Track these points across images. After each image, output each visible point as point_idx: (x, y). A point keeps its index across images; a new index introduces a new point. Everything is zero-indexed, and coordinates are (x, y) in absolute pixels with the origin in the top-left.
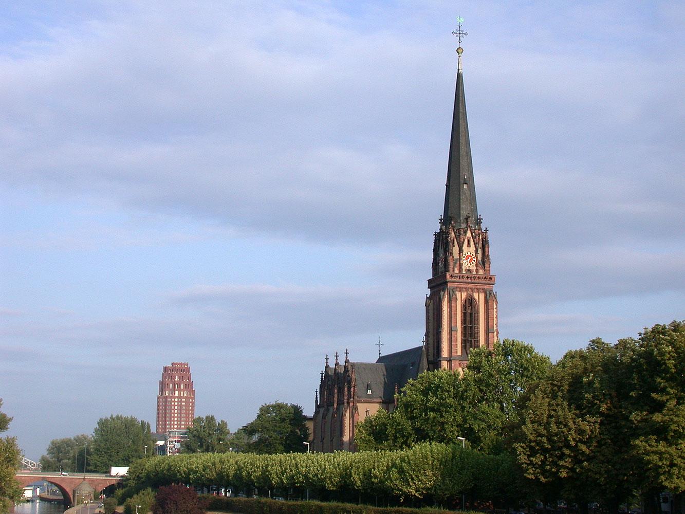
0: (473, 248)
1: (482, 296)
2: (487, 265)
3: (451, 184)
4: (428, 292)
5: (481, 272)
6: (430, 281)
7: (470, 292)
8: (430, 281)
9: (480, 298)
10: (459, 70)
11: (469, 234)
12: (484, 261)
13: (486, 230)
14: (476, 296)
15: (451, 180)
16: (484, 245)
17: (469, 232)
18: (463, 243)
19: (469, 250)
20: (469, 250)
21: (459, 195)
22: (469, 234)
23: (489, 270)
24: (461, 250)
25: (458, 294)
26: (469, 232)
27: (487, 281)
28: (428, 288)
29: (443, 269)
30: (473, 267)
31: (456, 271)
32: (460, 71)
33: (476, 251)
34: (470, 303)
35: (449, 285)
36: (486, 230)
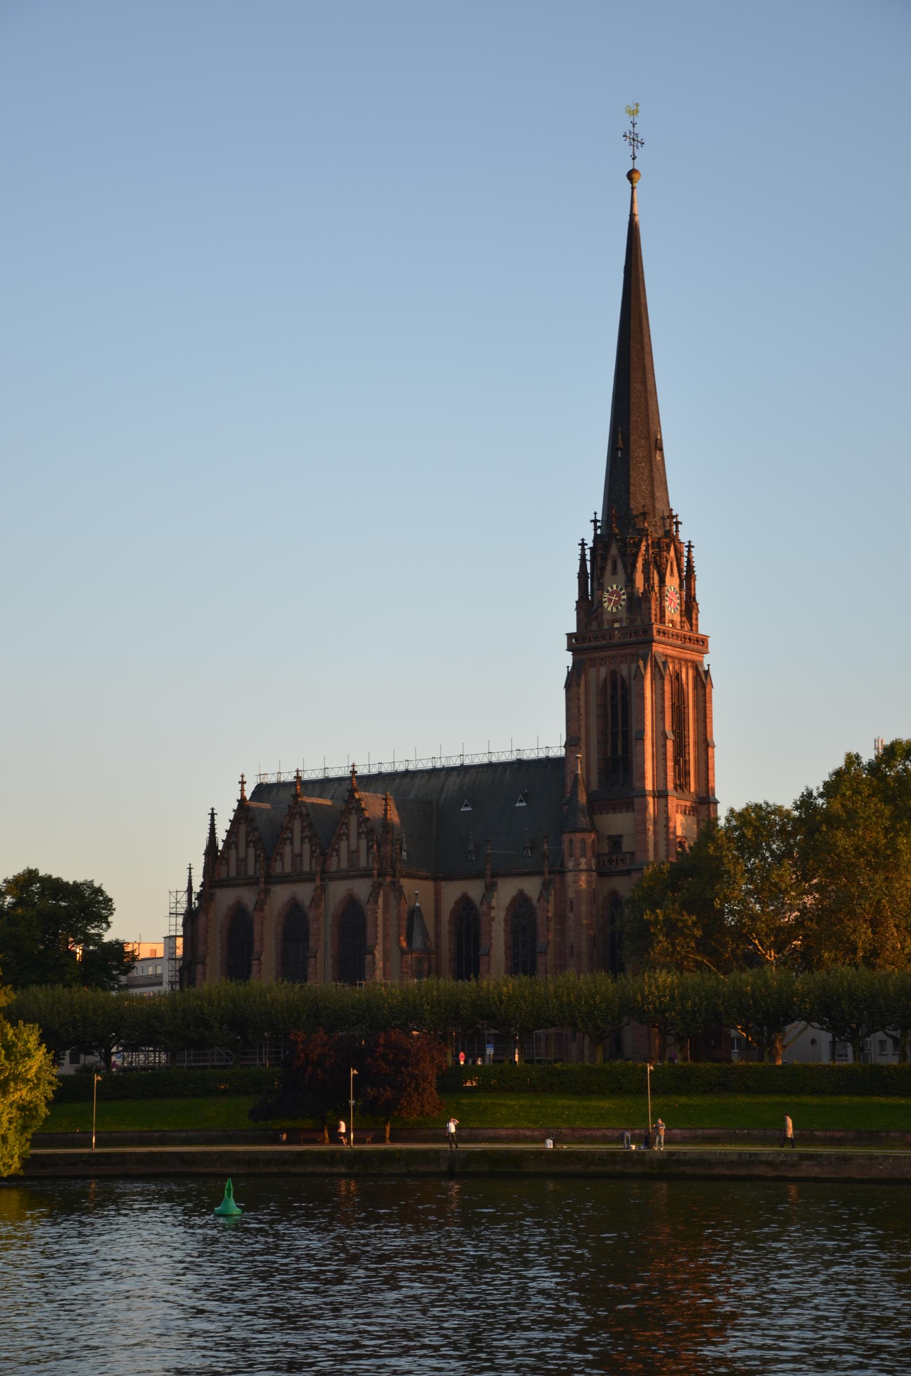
0: (676, 580)
3: (633, 446)
4: (568, 659)
6: (570, 636)
7: (677, 666)
8: (570, 636)
9: (687, 677)
10: (632, 215)
11: (672, 553)
15: (632, 438)
16: (688, 578)
21: (651, 470)
23: (697, 625)
24: (662, 581)
28: (568, 650)
30: (677, 618)
32: (637, 218)
33: (681, 586)
35: (657, 648)
36: (690, 547)
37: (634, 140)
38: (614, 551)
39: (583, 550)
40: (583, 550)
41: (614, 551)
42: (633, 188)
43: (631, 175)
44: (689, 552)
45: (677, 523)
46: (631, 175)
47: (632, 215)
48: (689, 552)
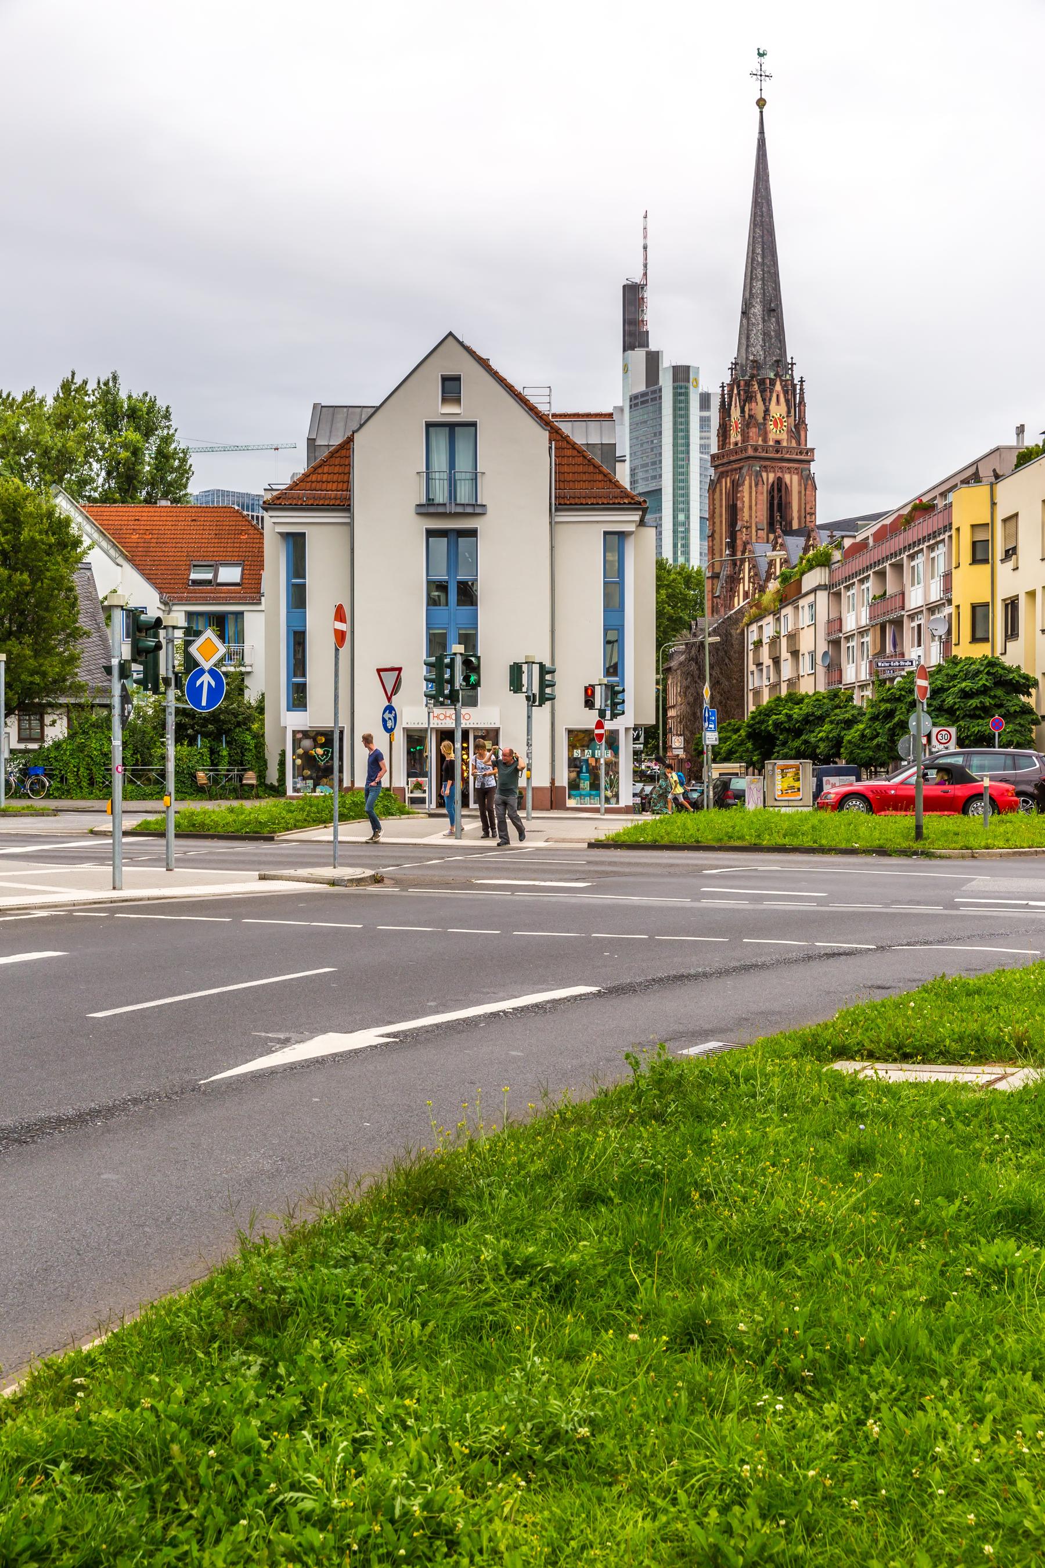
0: (783, 408)
1: (795, 478)
2: (802, 434)
5: (794, 444)
9: (792, 481)
10: (762, 132)
11: (778, 387)
12: (799, 428)
13: (802, 381)
14: (787, 478)
16: (795, 403)
17: (778, 383)
18: (770, 400)
19: (778, 410)
20: (778, 410)
22: (778, 387)
25: (764, 475)
26: (778, 383)
27: (802, 457)
29: (739, 438)
30: (784, 436)
31: (760, 442)
33: (789, 412)
34: (778, 490)
36: (802, 381)
37: (761, 75)
38: (735, 391)
39: (723, 391)
40: (723, 391)
41: (735, 391)
42: (761, 112)
43: (761, 103)
44: (802, 385)
45: (792, 364)
46: (761, 103)
47: (762, 132)
48: (802, 385)
